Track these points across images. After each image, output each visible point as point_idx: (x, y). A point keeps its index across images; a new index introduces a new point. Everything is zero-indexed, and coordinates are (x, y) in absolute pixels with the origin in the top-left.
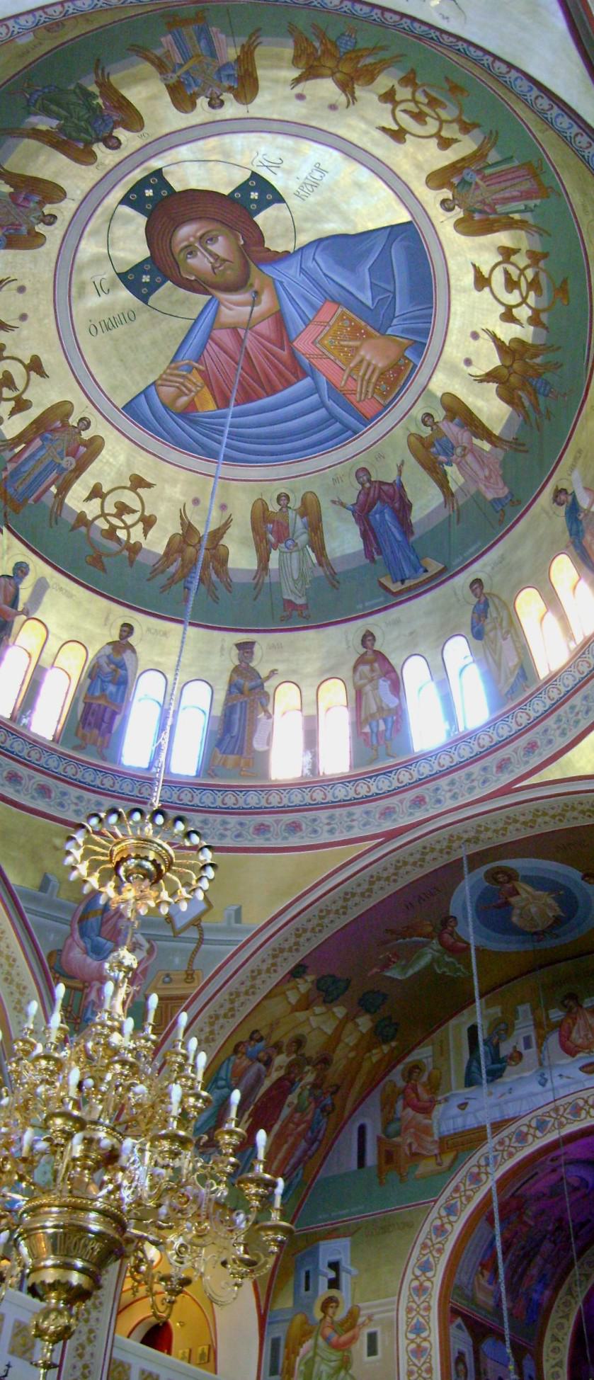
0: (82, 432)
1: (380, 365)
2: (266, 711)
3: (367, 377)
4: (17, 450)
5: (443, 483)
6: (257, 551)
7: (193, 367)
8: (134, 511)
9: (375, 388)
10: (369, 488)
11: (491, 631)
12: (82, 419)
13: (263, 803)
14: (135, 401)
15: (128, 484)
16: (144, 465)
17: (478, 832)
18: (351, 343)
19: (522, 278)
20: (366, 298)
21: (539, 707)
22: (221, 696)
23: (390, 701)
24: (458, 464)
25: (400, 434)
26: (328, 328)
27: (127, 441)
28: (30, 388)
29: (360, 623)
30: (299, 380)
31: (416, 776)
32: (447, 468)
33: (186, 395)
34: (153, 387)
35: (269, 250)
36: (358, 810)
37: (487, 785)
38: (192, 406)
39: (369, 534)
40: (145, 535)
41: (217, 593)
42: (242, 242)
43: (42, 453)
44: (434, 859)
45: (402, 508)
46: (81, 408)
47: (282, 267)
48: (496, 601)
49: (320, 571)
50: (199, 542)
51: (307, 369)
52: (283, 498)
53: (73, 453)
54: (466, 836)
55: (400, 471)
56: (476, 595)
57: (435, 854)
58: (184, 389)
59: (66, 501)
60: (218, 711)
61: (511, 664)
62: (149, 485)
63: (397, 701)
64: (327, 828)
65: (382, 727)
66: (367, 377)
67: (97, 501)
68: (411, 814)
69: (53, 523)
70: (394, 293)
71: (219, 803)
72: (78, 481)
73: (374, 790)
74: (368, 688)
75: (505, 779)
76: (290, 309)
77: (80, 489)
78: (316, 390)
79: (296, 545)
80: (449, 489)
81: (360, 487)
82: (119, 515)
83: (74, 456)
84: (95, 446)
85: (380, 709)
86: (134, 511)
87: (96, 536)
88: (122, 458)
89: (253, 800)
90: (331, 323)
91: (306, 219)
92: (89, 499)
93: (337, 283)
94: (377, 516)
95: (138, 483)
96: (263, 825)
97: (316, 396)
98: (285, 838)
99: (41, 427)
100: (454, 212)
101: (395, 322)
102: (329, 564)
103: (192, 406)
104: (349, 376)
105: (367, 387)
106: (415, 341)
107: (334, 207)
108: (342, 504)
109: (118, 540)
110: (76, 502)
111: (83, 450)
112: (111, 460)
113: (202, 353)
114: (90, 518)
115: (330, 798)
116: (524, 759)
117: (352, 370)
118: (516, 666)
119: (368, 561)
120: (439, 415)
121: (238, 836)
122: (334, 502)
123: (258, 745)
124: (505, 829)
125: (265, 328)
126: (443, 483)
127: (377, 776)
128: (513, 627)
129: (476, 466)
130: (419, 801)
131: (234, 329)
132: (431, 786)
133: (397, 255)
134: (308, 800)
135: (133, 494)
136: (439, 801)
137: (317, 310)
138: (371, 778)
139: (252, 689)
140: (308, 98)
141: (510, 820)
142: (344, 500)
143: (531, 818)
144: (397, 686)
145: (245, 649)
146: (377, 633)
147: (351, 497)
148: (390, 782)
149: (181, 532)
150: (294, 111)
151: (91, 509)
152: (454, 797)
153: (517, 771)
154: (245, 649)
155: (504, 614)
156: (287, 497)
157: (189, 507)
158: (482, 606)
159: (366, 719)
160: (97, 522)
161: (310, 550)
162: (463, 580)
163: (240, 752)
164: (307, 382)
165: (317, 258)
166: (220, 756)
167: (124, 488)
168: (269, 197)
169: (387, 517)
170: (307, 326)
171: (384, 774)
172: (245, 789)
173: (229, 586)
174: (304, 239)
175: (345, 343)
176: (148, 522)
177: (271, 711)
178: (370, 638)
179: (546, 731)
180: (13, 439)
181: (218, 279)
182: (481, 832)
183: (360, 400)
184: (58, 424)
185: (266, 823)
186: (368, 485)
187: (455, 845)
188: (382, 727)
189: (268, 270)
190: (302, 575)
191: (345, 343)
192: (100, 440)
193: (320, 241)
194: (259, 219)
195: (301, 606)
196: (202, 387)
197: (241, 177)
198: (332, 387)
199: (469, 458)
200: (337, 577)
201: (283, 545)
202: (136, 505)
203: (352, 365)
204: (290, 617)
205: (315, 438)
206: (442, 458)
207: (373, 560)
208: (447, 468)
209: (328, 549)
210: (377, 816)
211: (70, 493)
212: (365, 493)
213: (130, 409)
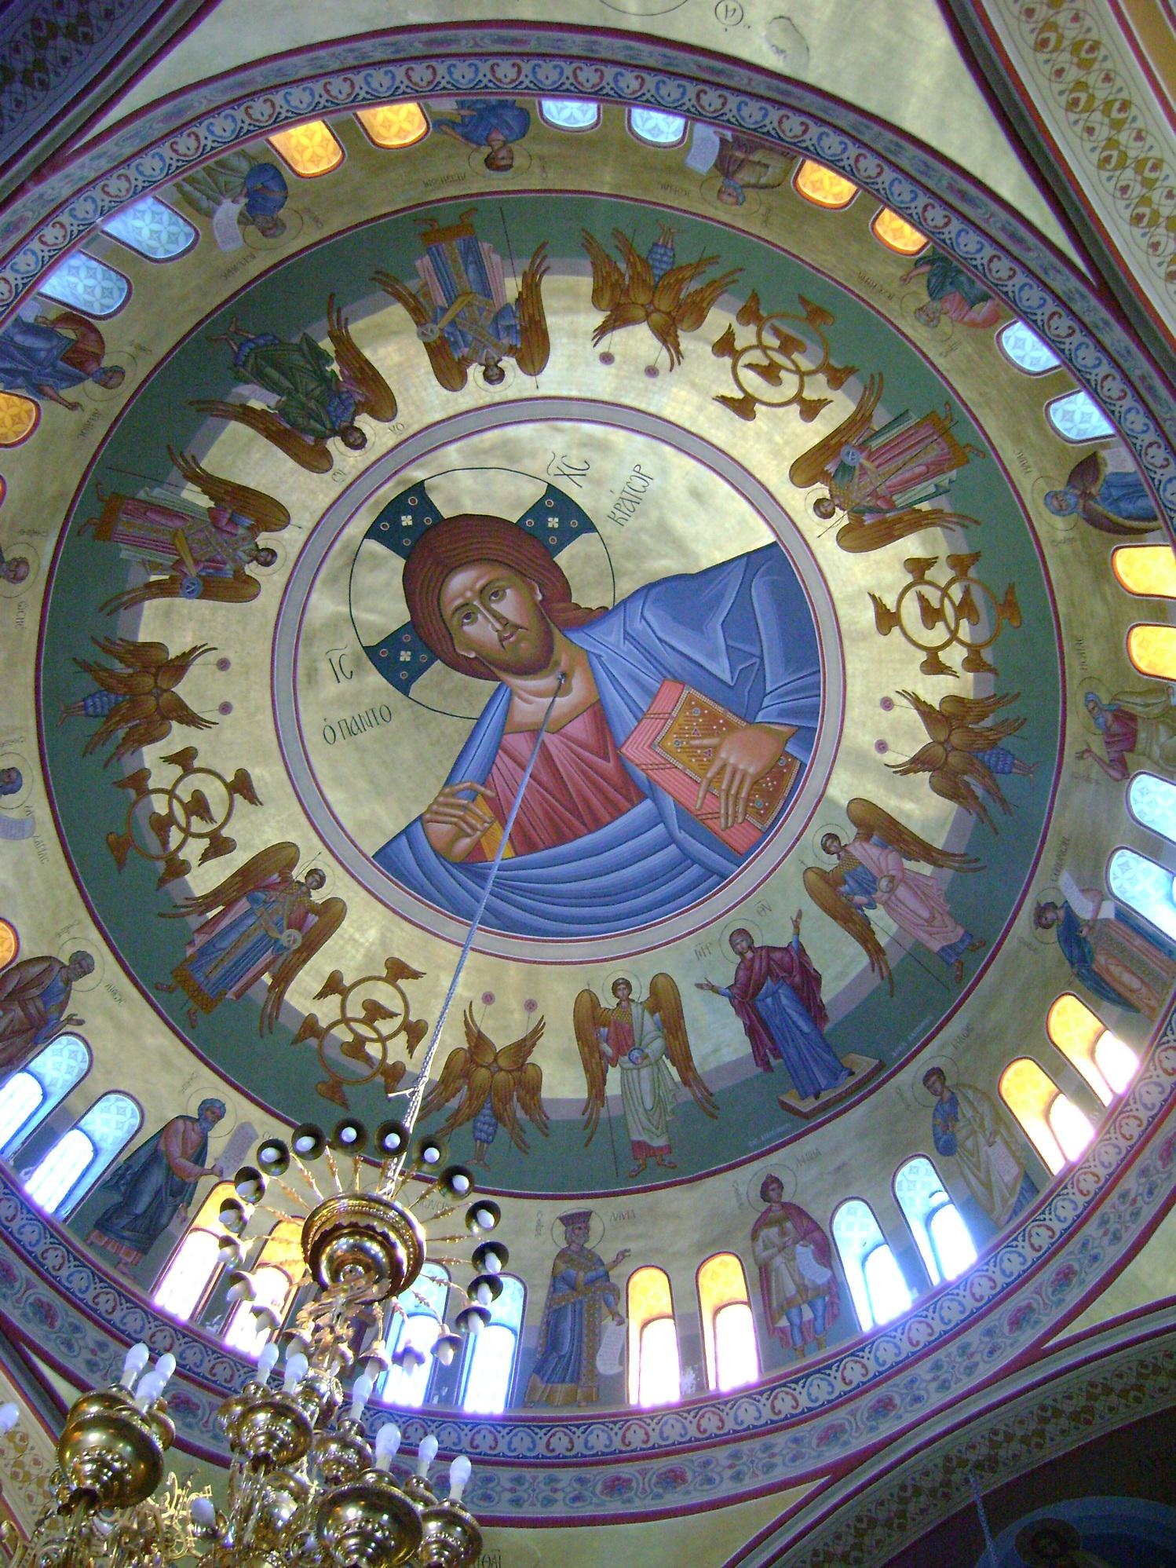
0: (313, 892)
1: (751, 770)
2: (614, 1314)
3: (733, 792)
4: (210, 915)
5: (865, 935)
6: (587, 1070)
7: (477, 792)
8: (392, 1015)
9: (747, 806)
10: (752, 960)
11: (967, 1138)
12: (313, 872)
13: (617, 1444)
14: (394, 845)
15: (384, 973)
16: (407, 944)
17: (993, 1444)
18: (706, 742)
20: (722, 669)
21: (1065, 1211)
22: (541, 1296)
23: (819, 1275)
24: (886, 904)
25: (791, 870)
26: (670, 722)
27: (380, 907)
28: (233, 820)
29: (755, 1166)
30: (634, 806)
31: (873, 1368)
33: (468, 835)
34: (419, 824)
35: (578, 607)
36: (780, 1440)
37: (996, 1355)
39: (757, 1029)
40: (411, 1052)
41: (526, 1137)
42: (540, 597)
43: (250, 921)
44: (923, 1511)
45: (806, 983)
46: (311, 855)
47: (597, 632)
48: (970, 1094)
49: (686, 1094)
50: (495, 1060)
51: (647, 792)
52: (621, 987)
53: (298, 924)
54: (973, 1457)
55: (797, 927)
56: (935, 1093)
57: (923, 1500)
58: (465, 826)
59: (287, 997)
60: (537, 1319)
61: (1008, 1178)
62: (416, 975)
63: (829, 1273)
64: (729, 1473)
65: (808, 1314)
66: (733, 792)
67: (335, 999)
68: (872, 1429)
69: (266, 1030)
70: (762, 659)
71: (541, 1449)
72: (307, 967)
73: (804, 1402)
74: (779, 1261)
75: (1027, 1337)
76: (613, 698)
77: (308, 979)
78: (660, 818)
79: (646, 1057)
81: (738, 959)
82: (369, 1021)
83: (300, 929)
84: (332, 915)
85: (802, 1289)
86: (392, 1015)
87: (333, 1053)
88: (373, 934)
89: (599, 1440)
90: (674, 714)
91: (629, 556)
92: (322, 995)
93: (682, 654)
94: (769, 1000)
95: (398, 971)
96: (618, 1479)
97: (661, 826)
98: (658, 1496)
99: (248, 879)
101: (767, 701)
102: (699, 1081)
104: (708, 791)
105: (736, 804)
106: (800, 728)
107: (664, 531)
108: (714, 989)
109: (368, 1059)
110: (302, 1000)
111: (313, 919)
112: (357, 936)
113: (490, 771)
114: (323, 1024)
115: (730, 1425)
116: (1055, 1299)
117: (710, 781)
118: (1016, 1179)
119: (760, 1070)
120: (848, 833)
121: (577, 1498)
122: (699, 986)
123: (604, 1365)
124: (1041, 1434)
125: (580, 728)
126: (865, 935)
127: (807, 1376)
128: (1004, 1120)
129: (912, 903)
130: (885, 1406)
131: (535, 732)
132: (901, 1379)
133: (760, 597)
134: (693, 1432)
135: (391, 988)
136: (917, 1399)
137: (654, 696)
138: (796, 1381)
139: (592, 1282)
140: (617, 359)
141: (1047, 1413)
143: (1083, 1402)
144: (826, 1251)
145: (577, 1223)
146: (785, 1178)
147: (725, 973)
148: (830, 1384)
149: (466, 1046)
150: (601, 383)
151: (326, 1011)
152: (944, 1386)
153: (1044, 1319)
154: (577, 1223)
155: (985, 1108)
156: (628, 984)
157: (478, 1005)
158: (946, 1107)
159: (781, 1306)
160: (335, 1031)
161: (668, 1063)
163: (576, 1378)
164: (647, 804)
165: (647, 614)
166: (541, 1386)
167: (379, 979)
168: (574, 523)
169: (784, 1001)
170: (639, 721)
171: (818, 1371)
172: (585, 1423)
173: (544, 1127)
174: (627, 587)
175: (696, 742)
176: (415, 1032)
177: (623, 1312)
178: (774, 1186)
179: (1085, 1245)
180: (205, 897)
181: (507, 657)
182: (999, 1445)
184: (276, 877)
185: (624, 1476)
186: (749, 955)
187: (956, 1478)
188: (808, 1314)
189: (577, 637)
190: (659, 1101)
191: (696, 742)
192: (340, 906)
193: (650, 587)
194: (562, 559)
195: (660, 1149)
196: (492, 823)
197: (533, 492)
199: (902, 892)
200: (713, 1099)
201: (626, 1058)
202: (395, 1005)
203: (709, 775)
204: (643, 1168)
205: (666, 890)
206: (860, 899)
207: (768, 1067)
208: (869, 913)
209: (696, 1061)
210: (814, 1442)
211: (293, 985)
212: (746, 966)
213: (385, 857)
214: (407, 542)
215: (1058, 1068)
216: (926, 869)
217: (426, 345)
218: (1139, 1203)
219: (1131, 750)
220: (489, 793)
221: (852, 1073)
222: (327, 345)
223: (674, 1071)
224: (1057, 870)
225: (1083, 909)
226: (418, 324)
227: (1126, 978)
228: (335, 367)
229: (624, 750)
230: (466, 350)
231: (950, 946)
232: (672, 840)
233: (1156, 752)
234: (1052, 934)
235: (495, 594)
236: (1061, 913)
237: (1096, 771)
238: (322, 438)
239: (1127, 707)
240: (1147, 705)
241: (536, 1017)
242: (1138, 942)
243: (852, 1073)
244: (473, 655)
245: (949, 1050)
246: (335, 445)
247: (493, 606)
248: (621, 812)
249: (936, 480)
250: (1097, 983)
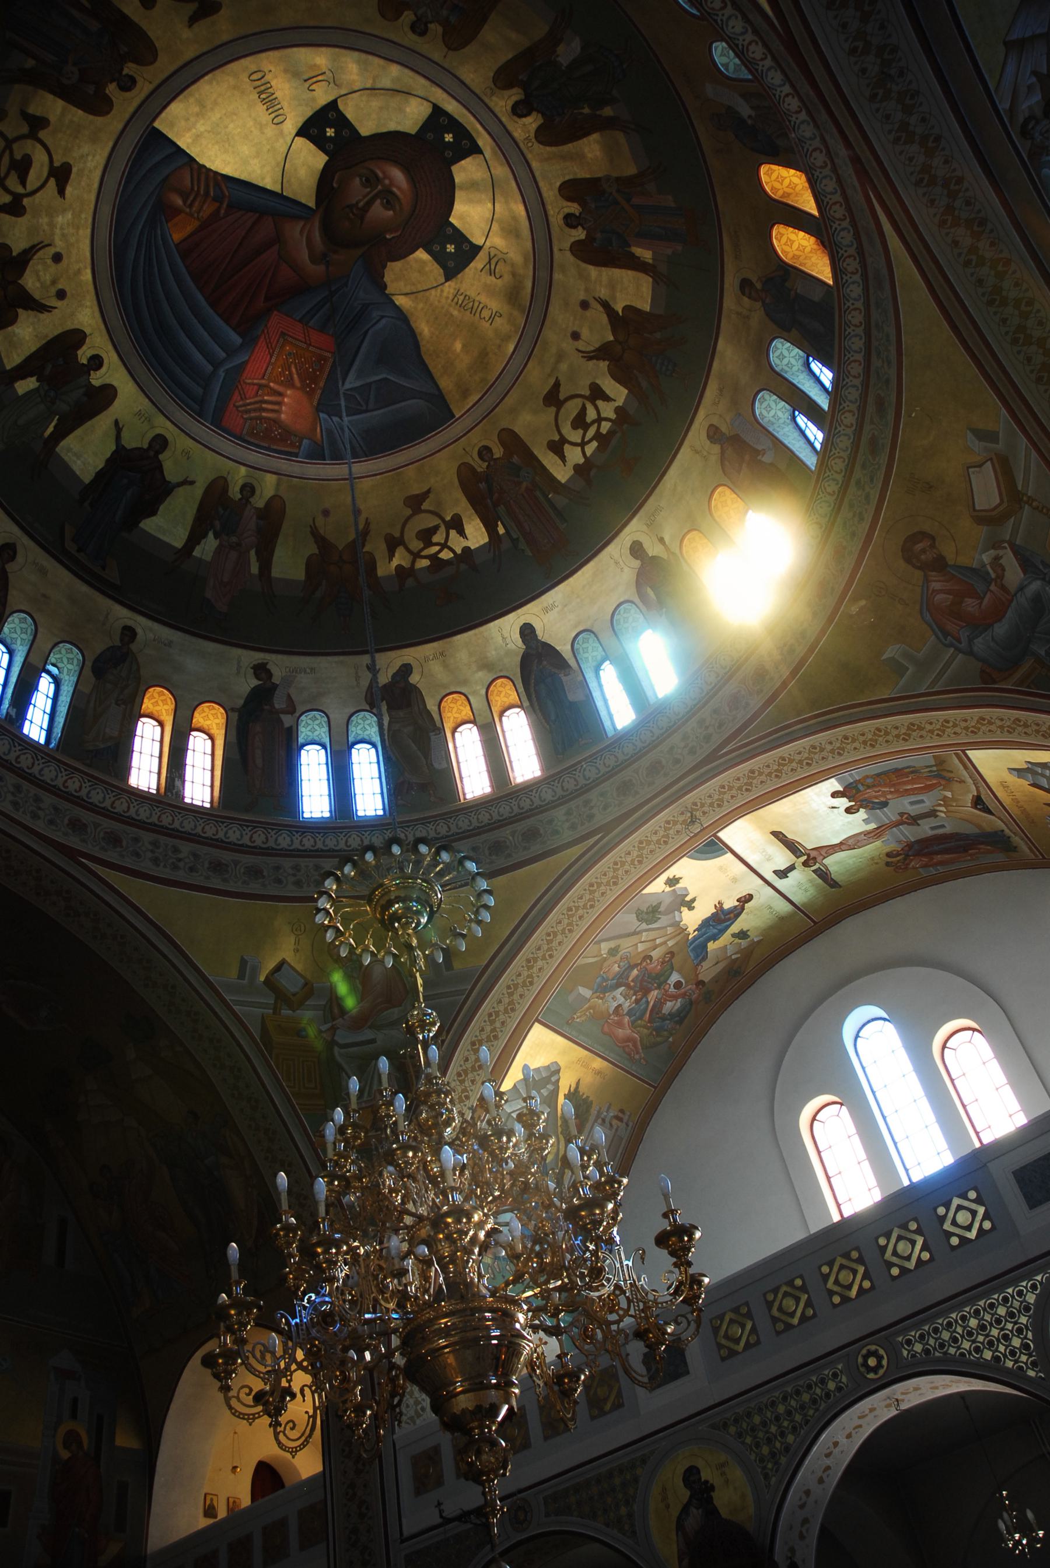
3: (264, 406)
9: (256, 418)
19: (437, 548)
26: (305, 346)
30: (234, 329)
32: (211, 535)
33: (185, 202)
35: (385, 267)
38: (173, 212)
58: (191, 198)
66: (264, 406)
67: (25, 129)
70: (366, 411)
75: (73, 841)
80: (193, 549)
84: (100, 106)
86: (23, 183)
90: (311, 348)
97: (223, 355)
100: (480, 462)
103: (173, 212)
104: (260, 386)
105: (255, 410)
106: (323, 447)
111: (91, 89)
122: (116, 422)
126: (195, 537)
142: (125, 435)
146: (20, 558)
147: (130, 441)
149: (14, 254)
157: (52, 251)
162: (122, 615)
164: (237, 339)
168: (451, 264)
175: (294, 370)
183: (237, 407)
186: (152, 453)
191: (294, 370)
194: (421, 255)
196: (198, 219)
198: (241, 368)
203: (272, 384)
208: (211, 535)
214: (430, 136)
216: (255, 569)
217: (599, 179)
220: (223, 211)
221: (104, 568)
222: (608, 111)
223: (51, 429)
226: (618, 179)
228: (586, 110)
229: (275, 312)
230: (593, 206)
232: (216, 365)
235: (388, 202)
237: (365, 683)
238: (525, 87)
241: (53, 302)
243: (104, 568)
244: (335, 185)
245: (151, 636)
246: (515, 95)
247: (378, 201)
248: (227, 321)
249: (521, 539)
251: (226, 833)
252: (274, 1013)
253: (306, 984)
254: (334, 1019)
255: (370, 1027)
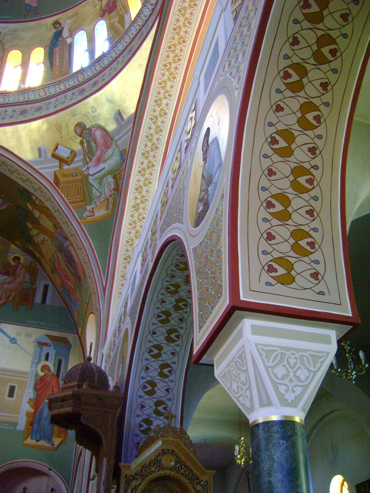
215: (25, 64)
218: (6, 117)
219: (109, 13)
224: (69, 18)
225: (65, 34)
227: (57, 60)
231: (30, 6)
233: (112, 21)
234: (54, 31)
236: (60, 29)
237: (98, 7)
239: (117, 4)
240: (120, 9)
242: (67, 56)
250: (51, 53)
251: (28, 97)
252: (60, 169)
253: (72, 152)
254: (88, 164)
255: (102, 163)
